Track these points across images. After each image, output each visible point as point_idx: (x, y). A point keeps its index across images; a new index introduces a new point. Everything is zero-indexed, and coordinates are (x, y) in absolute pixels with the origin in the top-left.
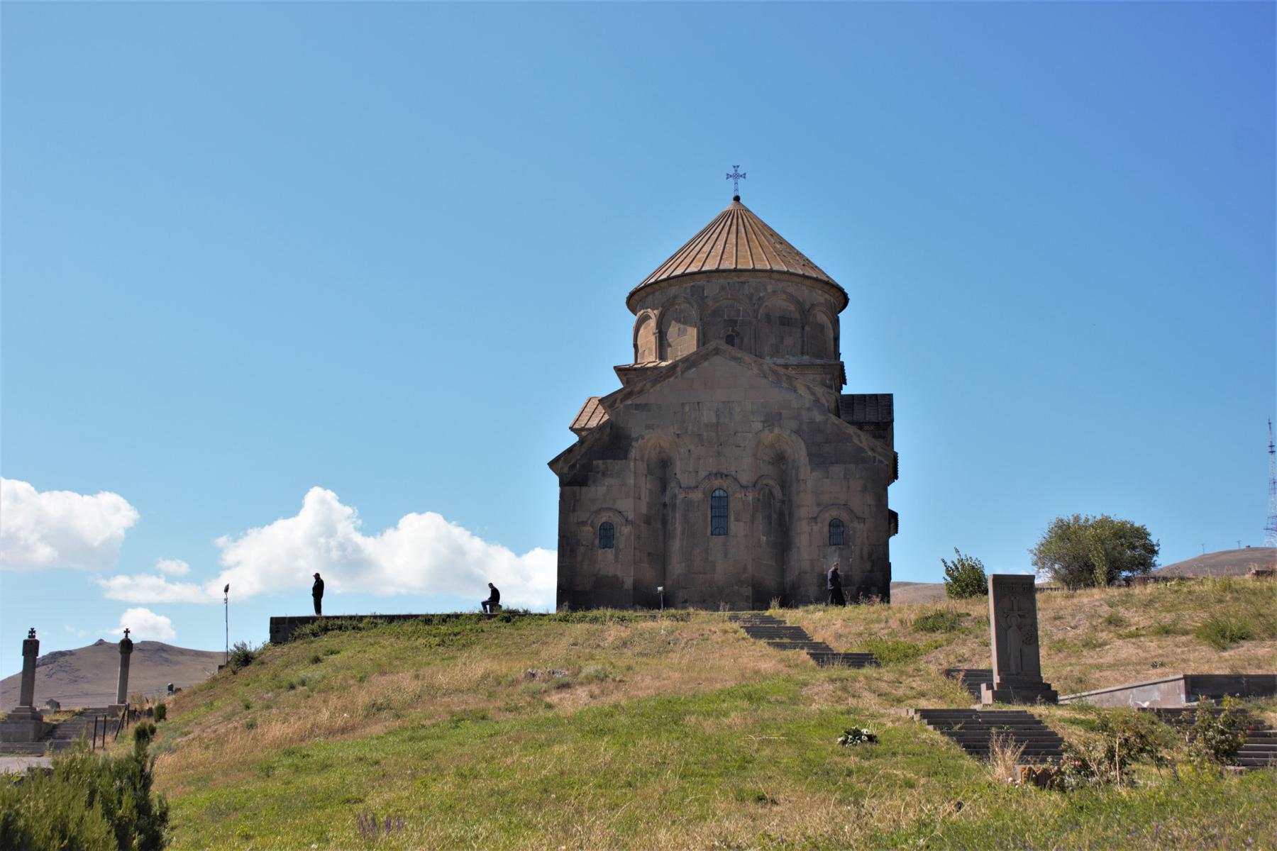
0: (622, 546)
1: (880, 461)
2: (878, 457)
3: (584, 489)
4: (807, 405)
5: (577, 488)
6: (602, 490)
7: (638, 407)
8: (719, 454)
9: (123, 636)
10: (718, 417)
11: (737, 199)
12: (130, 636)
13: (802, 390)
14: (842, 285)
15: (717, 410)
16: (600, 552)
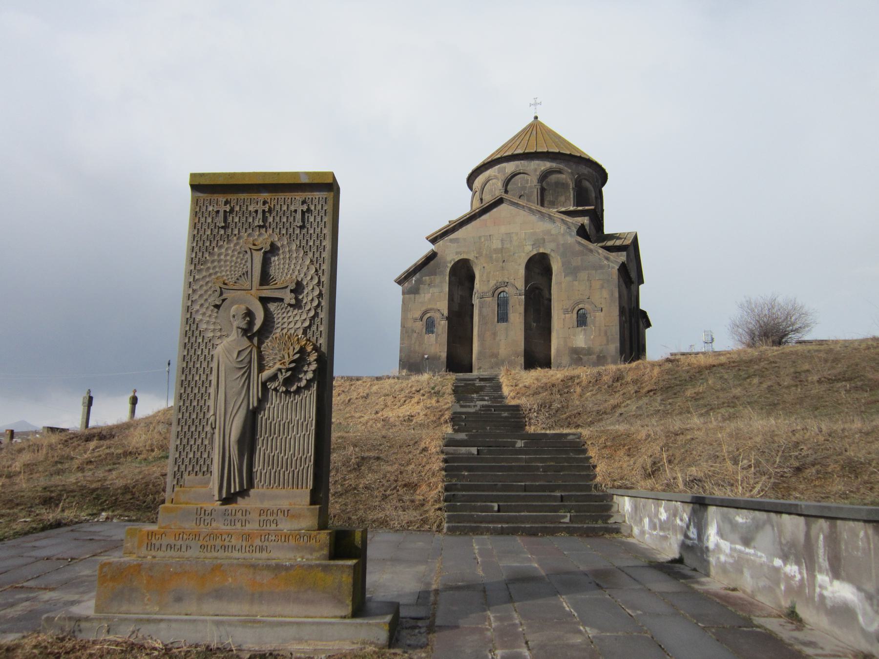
0: (440, 331)
1: (613, 268)
2: (611, 264)
3: (417, 296)
4: (562, 232)
5: (412, 296)
6: (428, 296)
7: (451, 241)
8: (503, 268)
9: (132, 394)
10: (503, 244)
11: (536, 118)
12: (137, 395)
13: (559, 224)
14: (600, 162)
15: (502, 240)
16: (426, 336)
